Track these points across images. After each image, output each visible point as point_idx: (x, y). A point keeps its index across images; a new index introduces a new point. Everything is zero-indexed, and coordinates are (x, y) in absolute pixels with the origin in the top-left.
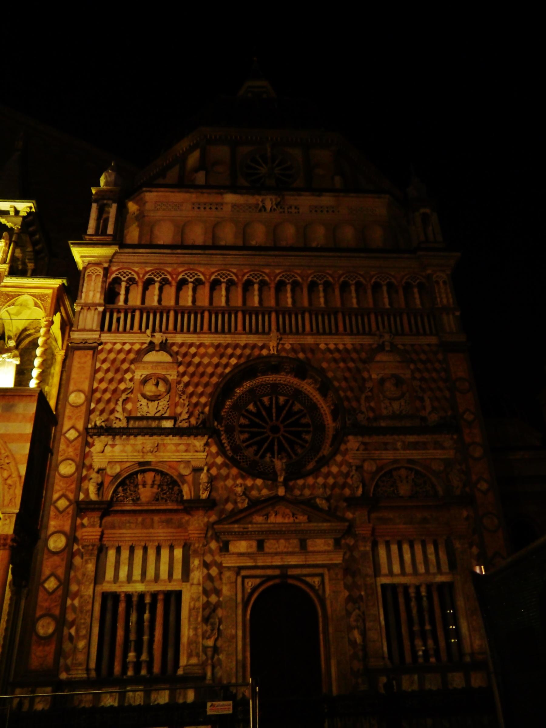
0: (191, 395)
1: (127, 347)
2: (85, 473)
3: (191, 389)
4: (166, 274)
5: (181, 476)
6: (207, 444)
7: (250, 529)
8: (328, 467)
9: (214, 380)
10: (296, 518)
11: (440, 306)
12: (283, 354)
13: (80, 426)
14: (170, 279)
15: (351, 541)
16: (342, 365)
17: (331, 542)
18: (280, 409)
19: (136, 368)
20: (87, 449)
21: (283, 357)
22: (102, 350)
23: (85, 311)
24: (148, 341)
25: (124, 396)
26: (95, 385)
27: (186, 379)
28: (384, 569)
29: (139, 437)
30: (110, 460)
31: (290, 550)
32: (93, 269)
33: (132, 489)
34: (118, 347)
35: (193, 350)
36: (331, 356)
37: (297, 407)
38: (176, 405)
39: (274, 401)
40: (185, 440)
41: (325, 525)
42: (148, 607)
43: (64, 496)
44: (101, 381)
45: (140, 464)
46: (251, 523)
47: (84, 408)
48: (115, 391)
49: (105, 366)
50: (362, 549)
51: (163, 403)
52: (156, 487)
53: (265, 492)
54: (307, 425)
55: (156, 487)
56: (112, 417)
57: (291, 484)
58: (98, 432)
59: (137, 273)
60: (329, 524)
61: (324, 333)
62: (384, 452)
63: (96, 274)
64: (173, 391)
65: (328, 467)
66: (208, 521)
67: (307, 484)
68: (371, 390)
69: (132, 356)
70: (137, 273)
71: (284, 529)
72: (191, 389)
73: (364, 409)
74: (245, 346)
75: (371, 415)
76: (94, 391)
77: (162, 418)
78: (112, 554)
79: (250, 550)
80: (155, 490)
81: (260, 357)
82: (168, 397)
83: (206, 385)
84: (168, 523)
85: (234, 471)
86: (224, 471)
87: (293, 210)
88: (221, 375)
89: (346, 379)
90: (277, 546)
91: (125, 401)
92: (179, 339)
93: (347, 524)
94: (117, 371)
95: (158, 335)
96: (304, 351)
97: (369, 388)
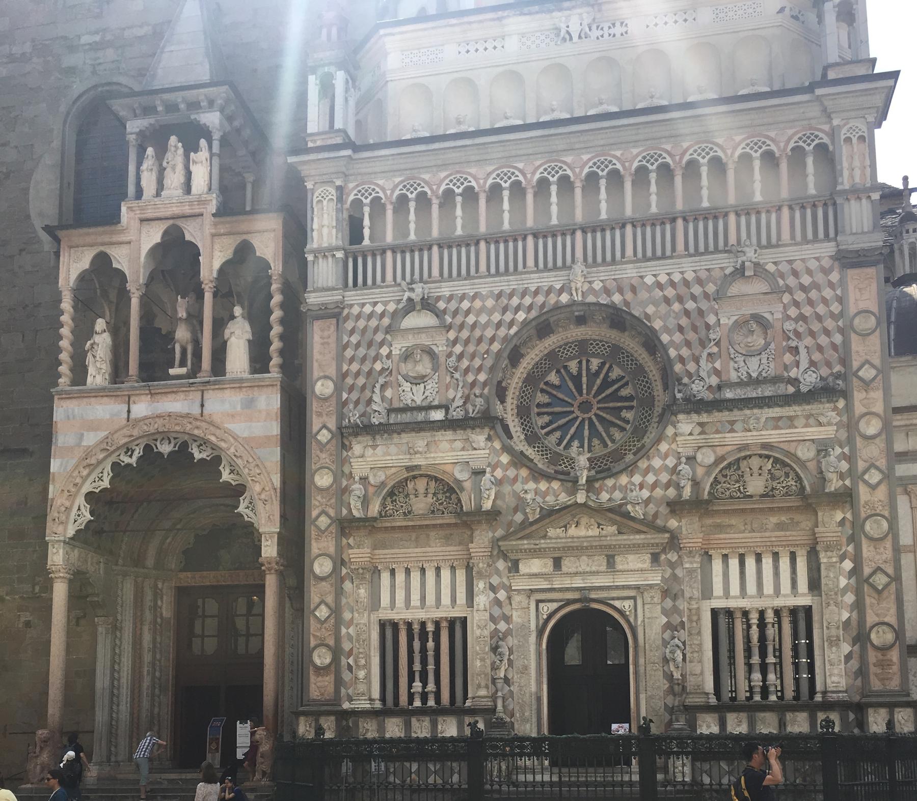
0: (467, 371)
1: (379, 309)
2: (345, 483)
3: (465, 363)
4: (423, 184)
5: (458, 482)
6: (489, 439)
7: (543, 546)
8: (648, 459)
9: (496, 347)
10: (602, 529)
11: (847, 187)
12: (591, 299)
13: (332, 425)
14: (429, 192)
15: (673, 557)
16: (676, 306)
17: (648, 557)
19: (393, 340)
20: (345, 454)
21: (589, 304)
22: (347, 318)
23: (321, 260)
24: (405, 298)
25: (381, 380)
26: (345, 367)
27: (458, 349)
28: (718, 589)
29: (403, 435)
30: (372, 466)
31: (594, 569)
32: (322, 192)
33: (402, 499)
34: (368, 309)
35: (466, 305)
36: (661, 294)
38: (447, 387)
40: (460, 434)
44: (352, 360)
45: (409, 469)
46: (545, 537)
47: (333, 401)
48: (369, 373)
49: (354, 339)
50: (687, 566)
51: (431, 385)
52: (430, 496)
53: (564, 498)
55: (430, 496)
56: (368, 409)
57: (597, 485)
58: (353, 432)
59: (383, 190)
60: (643, 536)
61: (654, 258)
62: (727, 435)
63: (327, 198)
64: (443, 368)
65: (648, 459)
66: (493, 536)
67: (618, 484)
68: (718, 344)
69: (386, 321)
70: (383, 190)
71: (585, 544)
72: (465, 363)
73: (703, 374)
74: (536, 293)
75: (714, 381)
76: (345, 375)
77: (430, 407)
79: (544, 570)
80: (430, 499)
81: (557, 307)
82: (436, 377)
84: (447, 539)
85: (524, 472)
86: (511, 473)
88: (506, 339)
89: (681, 329)
90: (578, 564)
91: (383, 387)
92: (445, 290)
93: (667, 535)
94: (370, 344)
95: (419, 288)
96: (620, 291)
97: (714, 340)
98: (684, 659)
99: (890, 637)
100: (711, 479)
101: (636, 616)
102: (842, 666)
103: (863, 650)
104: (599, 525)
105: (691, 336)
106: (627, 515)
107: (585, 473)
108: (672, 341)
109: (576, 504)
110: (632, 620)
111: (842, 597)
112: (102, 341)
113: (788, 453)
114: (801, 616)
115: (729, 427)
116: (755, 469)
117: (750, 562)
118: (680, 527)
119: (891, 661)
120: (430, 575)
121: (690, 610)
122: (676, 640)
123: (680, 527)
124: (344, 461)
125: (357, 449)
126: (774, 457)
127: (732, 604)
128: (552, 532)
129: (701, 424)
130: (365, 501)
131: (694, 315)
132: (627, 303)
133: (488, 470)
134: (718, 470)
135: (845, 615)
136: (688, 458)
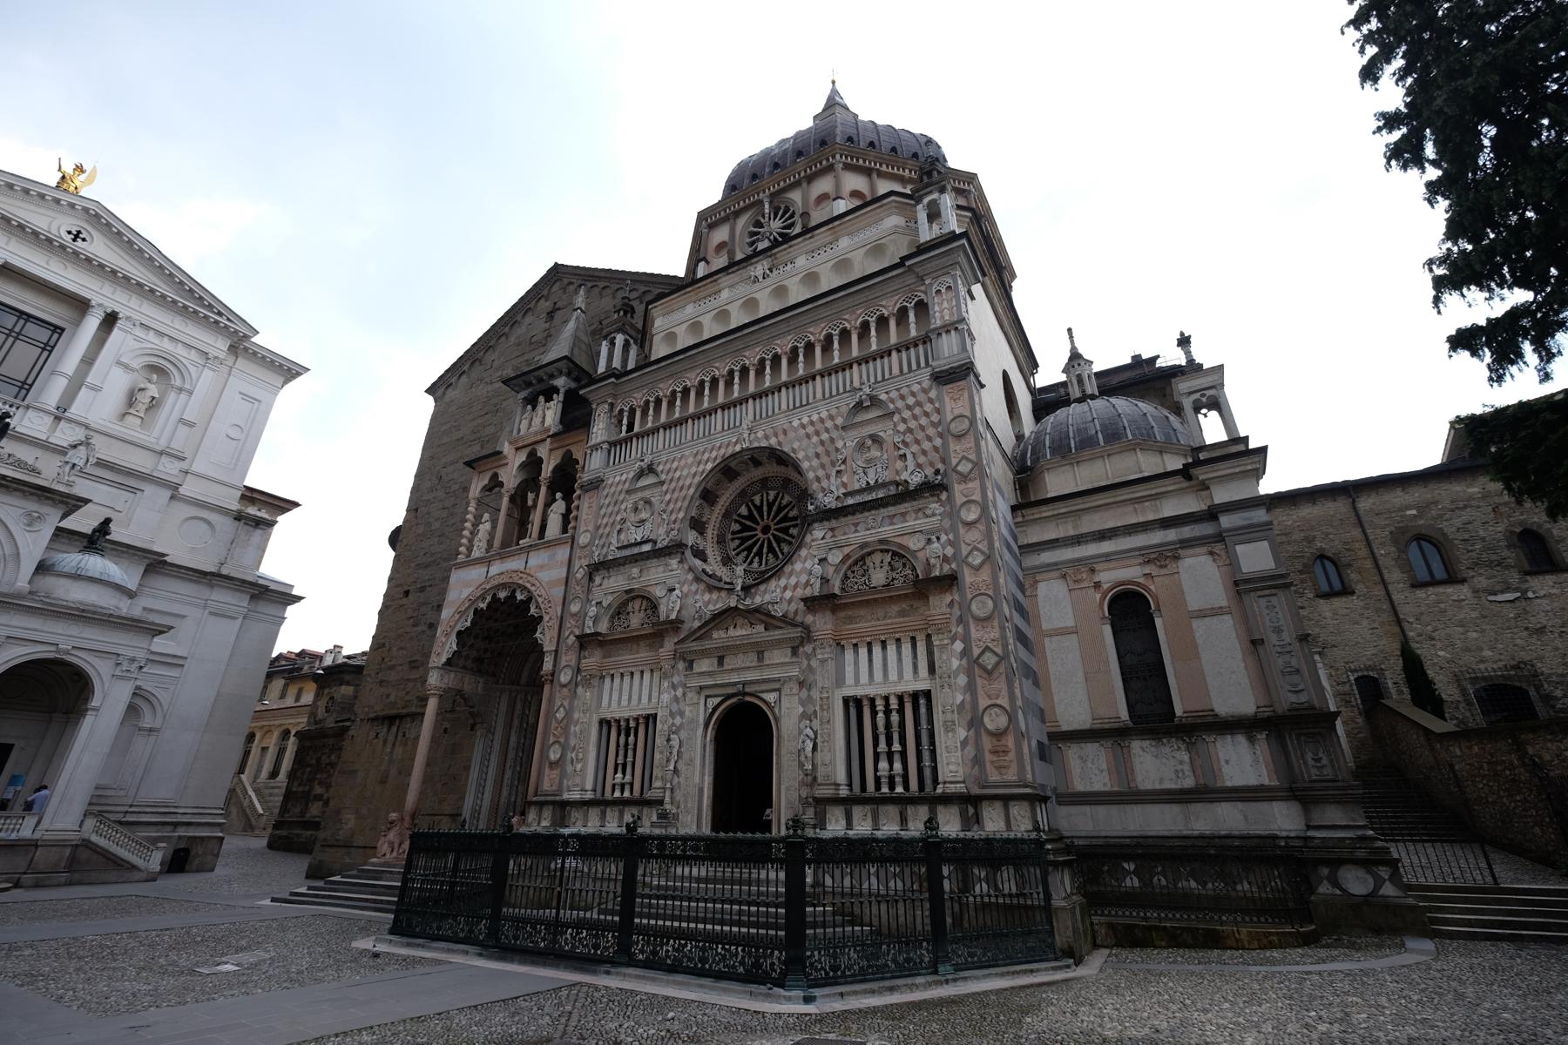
0: (671, 512)
1: (624, 478)
3: (672, 506)
9: (692, 490)
12: (756, 444)
15: (808, 648)
16: (815, 439)
17: (789, 651)
18: (770, 505)
21: (753, 448)
22: (604, 489)
25: (618, 527)
27: (668, 497)
31: (748, 664)
34: (618, 479)
37: (787, 499)
39: (765, 499)
41: (777, 634)
42: (632, 731)
43: (572, 632)
45: (627, 592)
48: (613, 524)
50: (819, 657)
51: (648, 525)
54: (795, 519)
57: (753, 591)
73: (833, 488)
74: (720, 447)
76: (599, 527)
78: (608, 680)
79: (711, 669)
81: (734, 455)
83: (684, 498)
85: (702, 586)
86: (694, 587)
87: (790, 266)
89: (817, 455)
93: (800, 629)
96: (776, 435)
98: (815, 748)
99: (1002, 721)
100: (841, 574)
101: (780, 707)
102: (959, 754)
103: (977, 734)
104: (752, 624)
105: (825, 460)
106: (769, 615)
107: (740, 581)
108: (811, 466)
109: (729, 609)
110: (776, 710)
111: (955, 678)
112: (485, 527)
113: (901, 546)
114: (922, 701)
115: (853, 529)
116: (878, 564)
117: (877, 650)
118: (814, 622)
119: (1006, 746)
120: (637, 677)
121: (821, 699)
122: (808, 729)
123: (814, 622)
124: (589, 591)
125: (598, 580)
126: (893, 552)
127: (859, 692)
128: (715, 635)
129: (832, 530)
130: (596, 620)
131: (827, 443)
132: (780, 443)
133: (677, 586)
134: (845, 567)
135: (959, 698)
136: (820, 560)
